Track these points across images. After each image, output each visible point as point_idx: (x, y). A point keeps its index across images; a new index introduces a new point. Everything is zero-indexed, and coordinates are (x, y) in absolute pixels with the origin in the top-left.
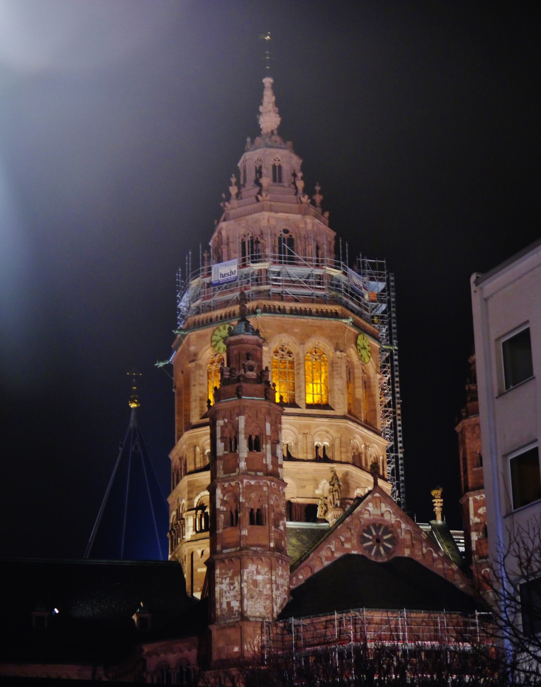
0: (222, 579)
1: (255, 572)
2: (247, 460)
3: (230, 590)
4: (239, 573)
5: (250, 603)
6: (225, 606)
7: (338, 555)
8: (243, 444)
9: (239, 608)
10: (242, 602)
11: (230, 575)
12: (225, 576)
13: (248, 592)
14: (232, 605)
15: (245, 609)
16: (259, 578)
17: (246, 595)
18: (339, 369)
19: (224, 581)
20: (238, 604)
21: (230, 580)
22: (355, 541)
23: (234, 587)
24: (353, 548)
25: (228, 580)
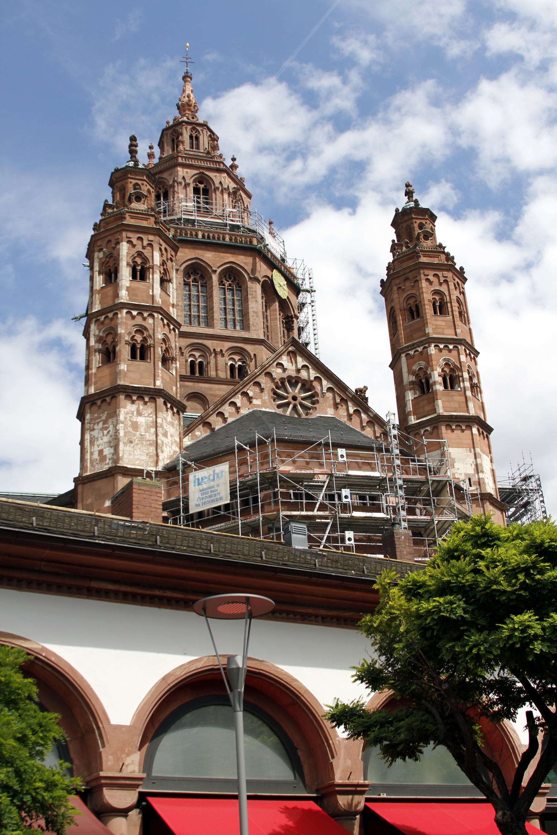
0: (94, 424)
1: (135, 413)
2: (128, 289)
3: (103, 435)
4: (114, 414)
5: (128, 448)
6: (96, 456)
7: (244, 411)
8: (125, 273)
9: (113, 455)
10: (116, 448)
11: (104, 418)
12: (97, 421)
13: (125, 435)
14: (104, 454)
15: (121, 455)
16: (141, 420)
17: (121, 439)
18: (254, 293)
19: (96, 427)
20: (112, 450)
21: (103, 424)
22: (267, 396)
23: (109, 431)
24: (264, 404)
25: (101, 425)
